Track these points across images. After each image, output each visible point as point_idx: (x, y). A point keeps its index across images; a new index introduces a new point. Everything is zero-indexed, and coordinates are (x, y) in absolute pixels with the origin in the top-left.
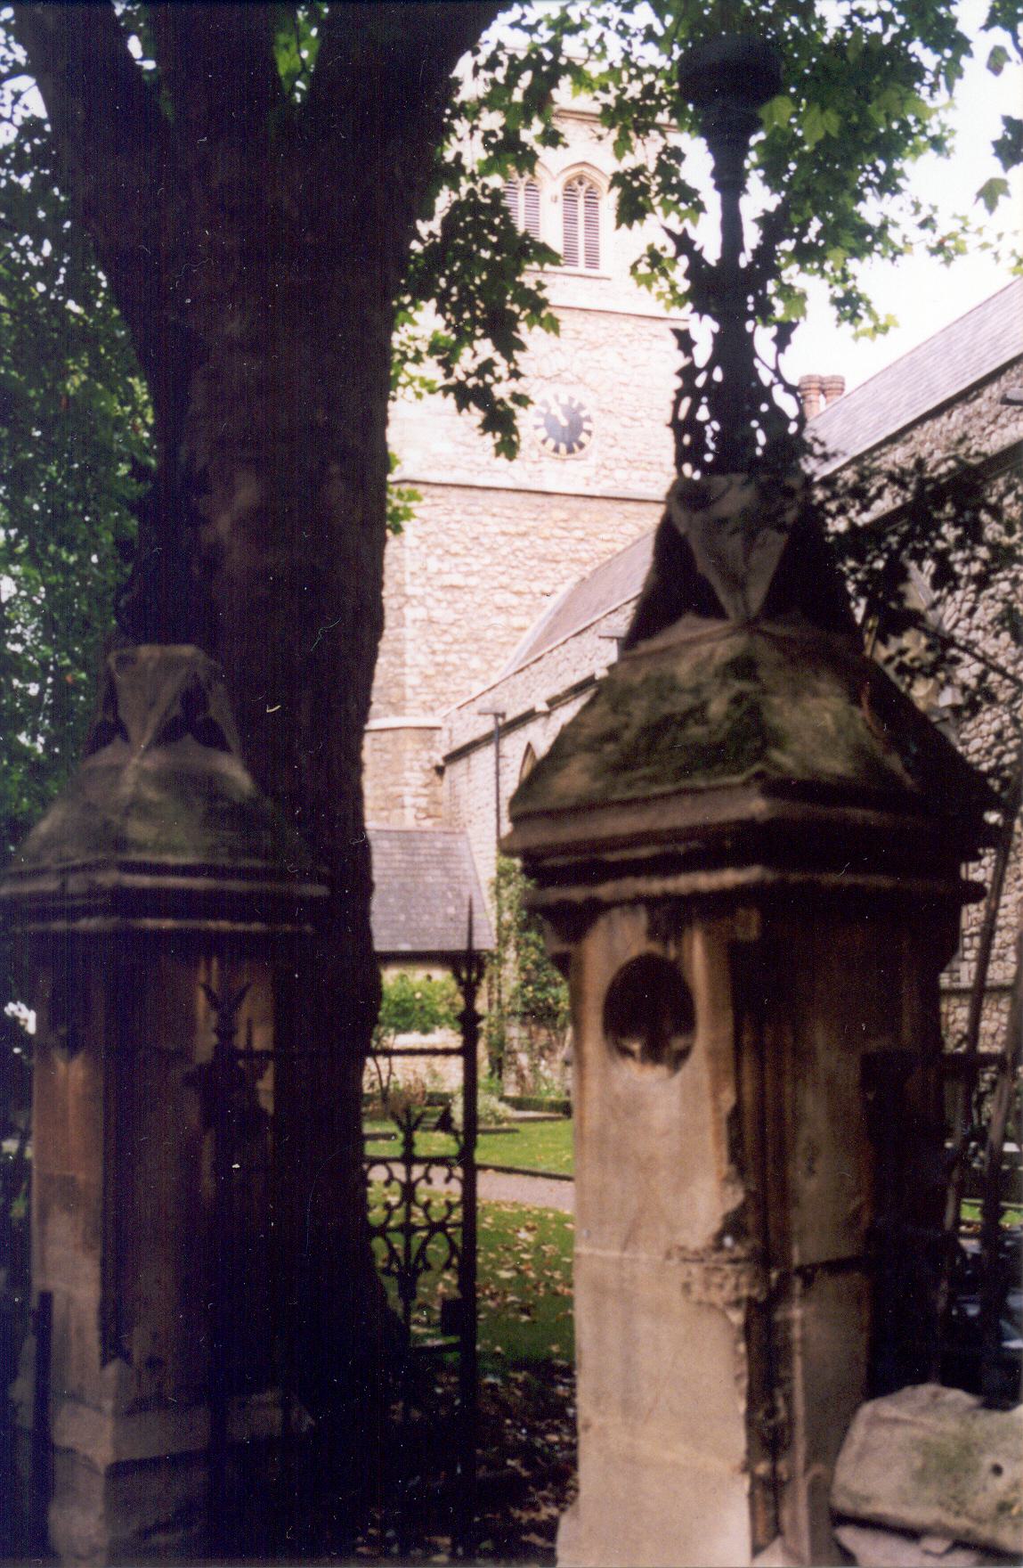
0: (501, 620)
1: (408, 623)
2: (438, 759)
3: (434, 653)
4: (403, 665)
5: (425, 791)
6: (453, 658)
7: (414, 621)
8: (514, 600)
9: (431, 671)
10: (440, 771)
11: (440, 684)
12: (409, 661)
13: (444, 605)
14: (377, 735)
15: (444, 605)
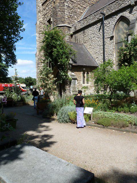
0: (79, 10)
1: (65, 6)
2: (71, 33)
3: (69, 13)
4: (65, 14)
5: (69, 39)
6: (72, 15)
7: (66, 6)
8: (81, 7)
9: (69, 16)
10: (72, 36)
11: (71, 19)
12: (66, 13)
13: (71, 4)
14: (59, 28)
15: (71, 4)
